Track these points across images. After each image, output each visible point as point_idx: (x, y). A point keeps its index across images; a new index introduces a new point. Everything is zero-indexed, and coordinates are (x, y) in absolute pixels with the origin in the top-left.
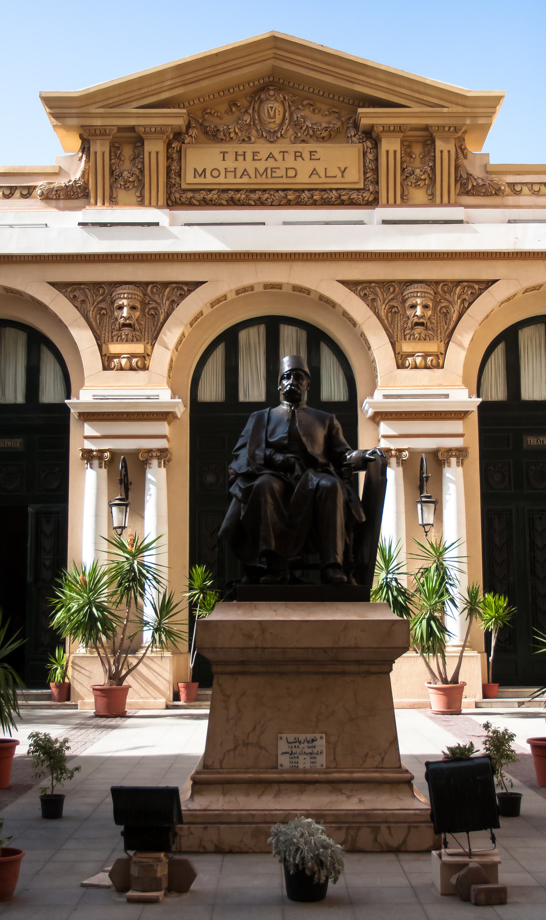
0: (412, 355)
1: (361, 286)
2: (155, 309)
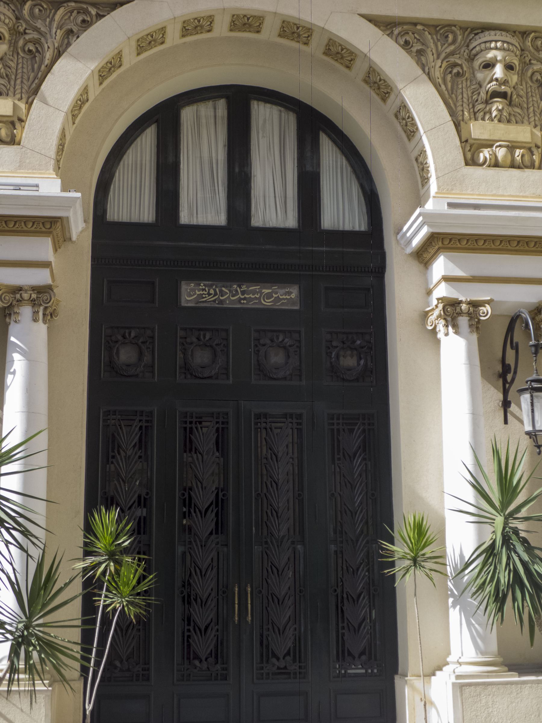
0: (489, 144)
1: (400, 29)
2: (36, 42)
